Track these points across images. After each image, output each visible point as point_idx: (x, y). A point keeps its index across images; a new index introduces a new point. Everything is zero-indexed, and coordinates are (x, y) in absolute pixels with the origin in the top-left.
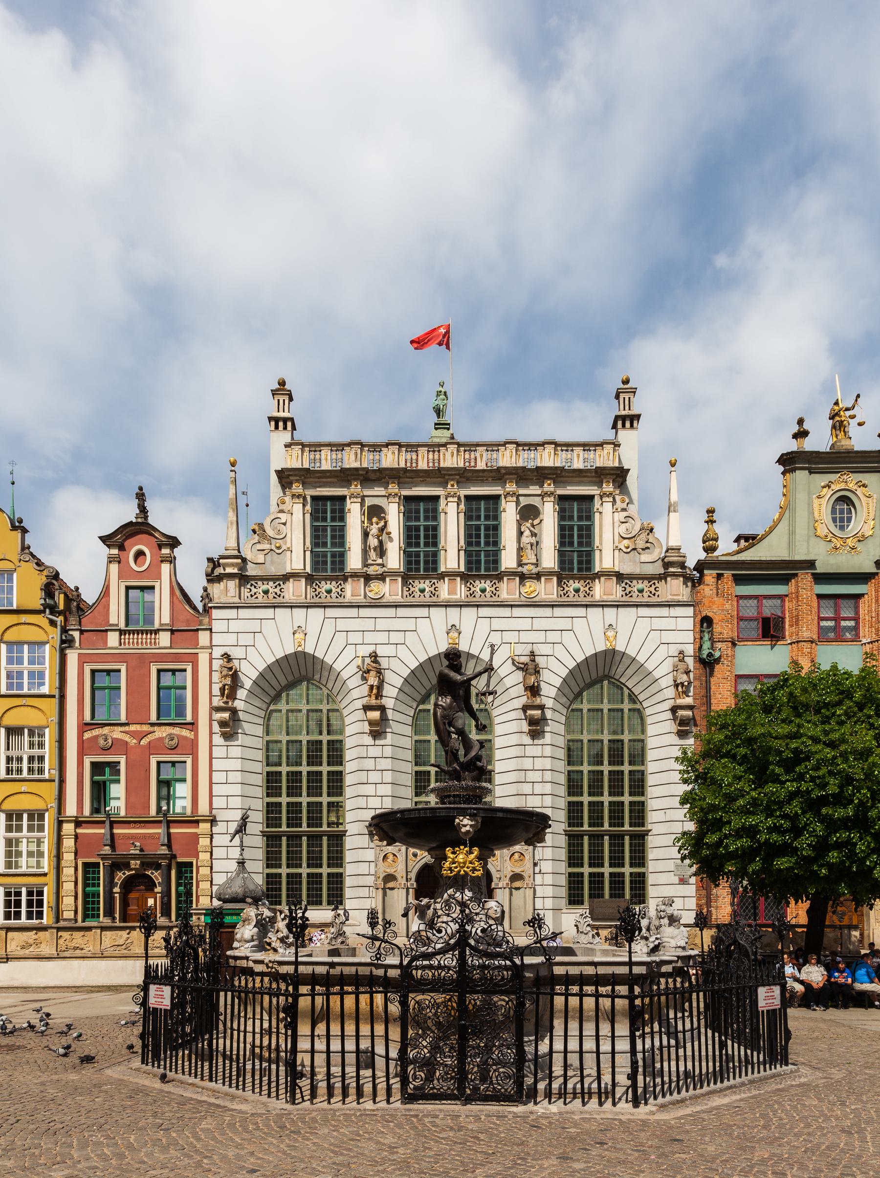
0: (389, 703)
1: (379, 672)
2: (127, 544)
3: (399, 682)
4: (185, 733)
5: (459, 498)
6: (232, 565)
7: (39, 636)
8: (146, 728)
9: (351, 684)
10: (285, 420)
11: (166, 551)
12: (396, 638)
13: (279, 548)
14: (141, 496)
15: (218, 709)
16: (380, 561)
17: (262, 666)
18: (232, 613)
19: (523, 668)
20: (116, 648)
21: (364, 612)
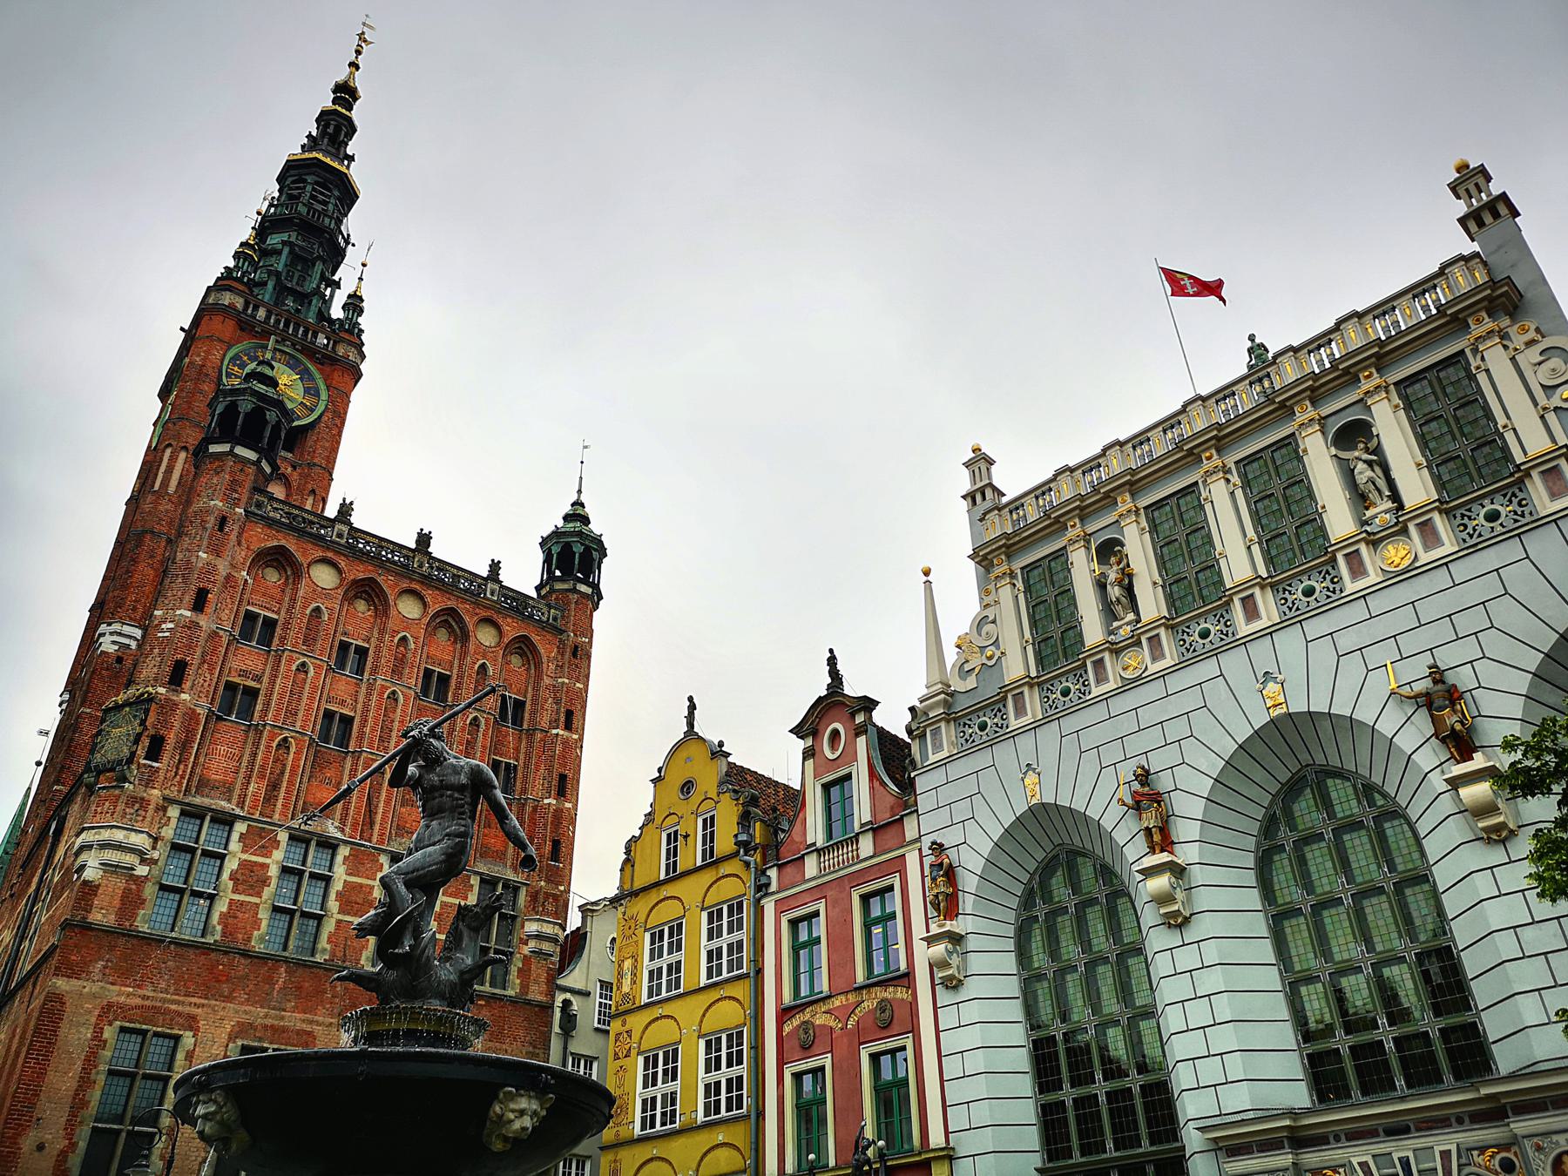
0: (1186, 854)
1: (1157, 798)
2: (821, 727)
3: (1197, 808)
4: (901, 994)
5: (1229, 471)
6: (937, 704)
7: (729, 889)
8: (852, 998)
9: (1120, 837)
10: (982, 491)
11: (860, 718)
12: (1176, 730)
13: (990, 658)
14: (832, 661)
15: (930, 940)
16: (1131, 616)
17: (986, 847)
18: (937, 777)
19: (1426, 701)
20: (814, 878)
21: (1118, 705)
